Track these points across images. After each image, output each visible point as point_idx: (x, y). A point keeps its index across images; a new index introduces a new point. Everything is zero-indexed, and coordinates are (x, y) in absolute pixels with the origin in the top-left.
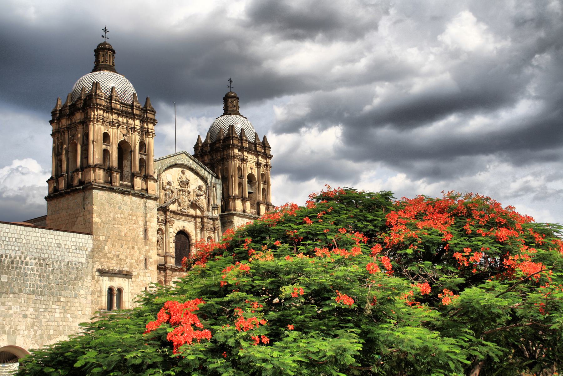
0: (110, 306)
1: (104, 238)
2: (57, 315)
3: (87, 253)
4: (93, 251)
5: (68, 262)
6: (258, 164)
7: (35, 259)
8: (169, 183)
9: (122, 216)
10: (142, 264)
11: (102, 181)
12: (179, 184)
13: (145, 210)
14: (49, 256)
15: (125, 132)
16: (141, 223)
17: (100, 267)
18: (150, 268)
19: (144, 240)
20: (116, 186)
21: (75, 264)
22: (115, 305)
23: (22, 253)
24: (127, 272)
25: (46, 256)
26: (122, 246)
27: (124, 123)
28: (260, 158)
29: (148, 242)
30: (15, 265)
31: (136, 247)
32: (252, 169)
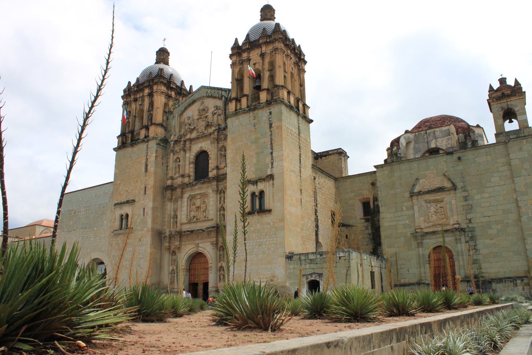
0: (121, 228)
1: (120, 181)
2: (92, 239)
3: (110, 195)
4: (112, 193)
5: (99, 205)
6: (262, 55)
7: (84, 208)
9: (132, 162)
10: (143, 192)
11: (120, 144)
12: (198, 115)
13: (147, 150)
15: (140, 103)
16: (144, 162)
17: (116, 202)
18: (147, 192)
19: (145, 173)
21: (103, 205)
22: (123, 226)
23: (79, 206)
24: (132, 200)
25: (89, 204)
27: (140, 98)
29: (148, 173)
30: (75, 214)
31: (139, 180)
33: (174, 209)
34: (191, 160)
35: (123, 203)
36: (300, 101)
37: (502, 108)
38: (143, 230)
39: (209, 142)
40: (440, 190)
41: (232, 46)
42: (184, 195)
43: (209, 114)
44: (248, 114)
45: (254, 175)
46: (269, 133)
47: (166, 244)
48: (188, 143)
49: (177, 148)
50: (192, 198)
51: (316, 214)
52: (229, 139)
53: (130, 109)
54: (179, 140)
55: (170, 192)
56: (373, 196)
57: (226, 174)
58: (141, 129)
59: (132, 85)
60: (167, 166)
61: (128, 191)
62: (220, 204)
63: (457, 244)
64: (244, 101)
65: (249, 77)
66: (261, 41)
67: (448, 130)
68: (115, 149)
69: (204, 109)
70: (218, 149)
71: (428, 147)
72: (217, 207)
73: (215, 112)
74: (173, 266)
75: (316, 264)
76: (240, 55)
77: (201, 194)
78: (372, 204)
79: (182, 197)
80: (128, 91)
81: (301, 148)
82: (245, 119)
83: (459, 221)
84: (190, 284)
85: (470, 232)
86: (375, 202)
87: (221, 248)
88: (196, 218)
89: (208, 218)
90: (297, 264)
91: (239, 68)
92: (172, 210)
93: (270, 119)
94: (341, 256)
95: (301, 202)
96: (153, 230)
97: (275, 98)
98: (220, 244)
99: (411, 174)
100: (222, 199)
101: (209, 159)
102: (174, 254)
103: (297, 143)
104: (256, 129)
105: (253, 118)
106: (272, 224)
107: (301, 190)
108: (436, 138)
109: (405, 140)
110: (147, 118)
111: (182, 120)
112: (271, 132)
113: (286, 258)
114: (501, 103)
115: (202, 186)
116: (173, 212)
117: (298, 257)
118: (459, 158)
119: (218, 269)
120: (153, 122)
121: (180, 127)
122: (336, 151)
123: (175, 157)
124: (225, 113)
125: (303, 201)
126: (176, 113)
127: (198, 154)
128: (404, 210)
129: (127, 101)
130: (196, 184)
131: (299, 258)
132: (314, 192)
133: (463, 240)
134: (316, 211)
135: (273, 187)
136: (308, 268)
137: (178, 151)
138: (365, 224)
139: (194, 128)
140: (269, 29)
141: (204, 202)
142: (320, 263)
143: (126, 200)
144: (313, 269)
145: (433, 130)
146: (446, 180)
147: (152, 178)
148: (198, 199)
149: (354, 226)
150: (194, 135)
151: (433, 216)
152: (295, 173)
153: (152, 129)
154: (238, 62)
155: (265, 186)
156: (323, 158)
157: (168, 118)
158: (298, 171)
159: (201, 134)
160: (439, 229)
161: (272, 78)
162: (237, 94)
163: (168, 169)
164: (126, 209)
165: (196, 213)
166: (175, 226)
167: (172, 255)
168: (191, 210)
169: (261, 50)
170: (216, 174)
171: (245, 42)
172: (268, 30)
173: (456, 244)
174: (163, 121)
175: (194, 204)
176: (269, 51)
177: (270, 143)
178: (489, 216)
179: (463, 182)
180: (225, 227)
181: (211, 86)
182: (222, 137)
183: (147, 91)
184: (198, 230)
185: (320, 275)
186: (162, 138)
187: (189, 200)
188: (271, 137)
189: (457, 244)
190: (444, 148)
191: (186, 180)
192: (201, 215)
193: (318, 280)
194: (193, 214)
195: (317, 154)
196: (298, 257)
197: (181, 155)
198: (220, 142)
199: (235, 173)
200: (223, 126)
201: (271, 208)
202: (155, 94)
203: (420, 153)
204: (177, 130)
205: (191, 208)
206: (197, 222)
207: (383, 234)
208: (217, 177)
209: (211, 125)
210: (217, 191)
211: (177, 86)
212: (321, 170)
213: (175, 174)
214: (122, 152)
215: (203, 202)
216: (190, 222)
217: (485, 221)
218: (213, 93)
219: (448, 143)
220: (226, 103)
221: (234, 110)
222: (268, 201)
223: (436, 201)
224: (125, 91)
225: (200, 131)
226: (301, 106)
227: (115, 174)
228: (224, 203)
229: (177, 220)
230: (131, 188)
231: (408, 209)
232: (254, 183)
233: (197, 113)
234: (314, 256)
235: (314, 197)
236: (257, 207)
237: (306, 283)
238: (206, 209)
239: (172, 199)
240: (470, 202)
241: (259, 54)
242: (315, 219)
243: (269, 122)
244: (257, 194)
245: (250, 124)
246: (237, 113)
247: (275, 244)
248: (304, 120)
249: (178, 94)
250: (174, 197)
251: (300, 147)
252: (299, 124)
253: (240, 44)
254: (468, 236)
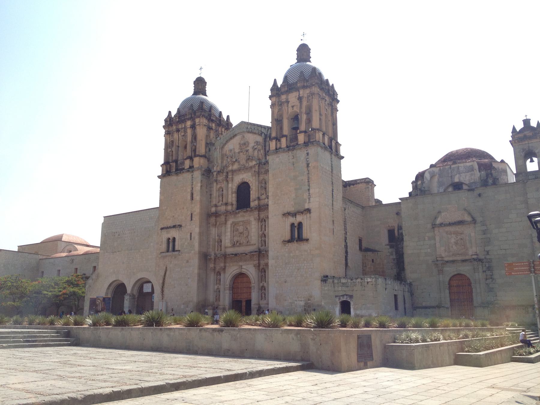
0: (168, 251)
1: (166, 207)
3: (155, 220)
5: (145, 228)
6: (300, 99)
7: (129, 230)
8: (231, 151)
9: (177, 189)
10: (189, 218)
11: (165, 172)
13: (192, 180)
14: (136, 227)
15: (183, 134)
16: (189, 190)
17: (162, 226)
19: (191, 201)
20: (173, 172)
21: (149, 229)
22: (171, 249)
23: (123, 229)
26: (176, 209)
27: (182, 129)
28: (301, 92)
29: (193, 201)
30: (120, 236)
32: (293, 107)
33: (218, 234)
34: (234, 190)
35: (170, 227)
36: (333, 140)
38: (191, 253)
39: (250, 174)
40: (461, 223)
41: (271, 86)
42: (227, 221)
43: (250, 148)
44: (287, 153)
45: (293, 208)
46: (306, 172)
47: (212, 265)
48: (230, 174)
49: (220, 178)
50: (234, 224)
51: (345, 241)
52: (270, 175)
53: (172, 139)
54: (222, 171)
55: (214, 218)
56: (398, 225)
57: (268, 205)
58: (186, 159)
59: (173, 116)
60: (211, 195)
61: (175, 217)
62: (261, 231)
63: (475, 272)
64: (284, 140)
65: (288, 118)
66: (298, 85)
67: (472, 165)
68: (159, 177)
69: (244, 143)
70: (259, 181)
71: (452, 181)
72: (259, 233)
73: (255, 147)
74: (218, 285)
75: (347, 287)
76: (279, 96)
77: (243, 221)
78: (397, 232)
79: (226, 223)
80: (170, 121)
81: (333, 183)
82: (284, 157)
83: (478, 252)
84: (233, 301)
85: (487, 263)
86: (400, 230)
87: (263, 271)
88: (239, 242)
89: (250, 243)
90: (331, 286)
91: (278, 109)
92: (216, 236)
93: (308, 160)
94: (368, 281)
95: (333, 231)
96: (200, 252)
97: (311, 140)
98: (261, 267)
99: (434, 207)
100: (263, 227)
101: (250, 190)
102: (219, 274)
103: (331, 180)
104: (294, 167)
105: (293, 157)
106: (309, 251)
107: (333, 221)
108: (460, 173)
109: (430, 175)
110: (190, 149)
111: (224, 152)
112: (309, 171)
113: (321, 280)
114: (522, 144)
115: (244, 214)
116: (217, 236)
117: (331, 280)
118: (480, 195)
119: (260, 287)
120: (197, 153)
121: (222, 158)
122: (364, 180)
123: (218, 186)
124: (265, 149)
125: (335, 230)
126: (218, 144)
127: (239, 185)
129: (169, 130)
130: (239, 212)
131: (333, 281)
132: (344, 222)
133: (481, 270)
134: (346, 239)
135: (310, 220)
136: (340, 290)
137: (221, 181)
138: (390, 250)
139: (236, 160)
140: (306, 73)
141: (247, 228)
142: (351, 287)
143: (173, 225)
144: (345, 291)
145: (457, 165)
146: (466, 215)
147: (198, 206)
148: (240, 225)
149: (379, 251)
150: (236, 167)
151: (454, 246)
152: (328, 207)
153: (196, 160)
154: (277, 103)
155: (303, 218)
156: (352, 186)
157: (210, 149)
158: (331, 205)
159: (243, 167)
160: (459, 258)
161: (309, 121)
162: (277, 133)
163: (212, 197)
164: (173, 233)
165: (239, 238)
166: (220, 249)
167: (217, 275)
168: (234, 235)
169: (299, 93)
170: (257, 204)
171: (283, 84)
172: (305, 74)
174: (206, 152)
175: (237, 230)
176: (307, 95)
177: (307, 181)
178: (505, 250)
179: (483, 217)
180: (267, 251)
181: (250, 122)
182: (263, 170)
183: (189, 123)
184: (242, 254)
185: (351, 297)
186: (206, 169)
187: (232, 226)
188: (308, 175)
190: (467, 182)
191: (229, 208)
192: (243, 240)
193: (349, 301)
194: (236, 239)
195: (345, 182)
196: (331, 280)
197: (224, 185)
198: (261, 175)
199: (276, 205)
200: (263, 161)
201: (308, 237)
202: (197, 127)
203: (444, 186)
204: (220, 162)
205: (234, 233)
206: (241, 246)
207: (406, 260)
208: (259, 208)
209: (252, 159)
210: (259, 219)
211: (216, 118)
212: (350, 201)
213: (219, 202)
214: (167, 179)
215: (246, 229)
216: (234, 245)
218: (253, 128)
219: (471, 179)
220: (265, 140)
221: (275, 148)
222: (305, 231)
223: (456, 233)
224: (166, 121)
225: (241, 163)
226: (333, 144)
227: (160, 200)
228: (265, 231)
229: (221, 244)
230: (177, 214)
231: (429, 239)
232: (293, 215)
233: (238, 146)
234: (345, 280)
235: (344, 226)
236: (296, 236)
237: (338, 303)
238: (248, 235)
239: (216, 224)
241: (297, 98)
242: (345, 245)
243: (306, 162)
244: (296, 224)
245: (289, 162)
246: (277, 152)
247: (312, 268)
248: (337, 158)
249: (218, 126)
250: (218, 223)
251: (332, 182)
252: (332, 162)
253: (279, 86)
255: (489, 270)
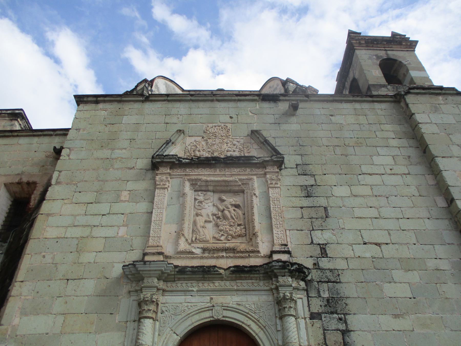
37: (378, 57)
63: (281, 318)
85: (325, 285)
128: (123, 198)
173: (278, 321)
189: (281, 318)
217: (368, 255)
240: (323, 202)
254: (320, 296)
255: (332, 313)
